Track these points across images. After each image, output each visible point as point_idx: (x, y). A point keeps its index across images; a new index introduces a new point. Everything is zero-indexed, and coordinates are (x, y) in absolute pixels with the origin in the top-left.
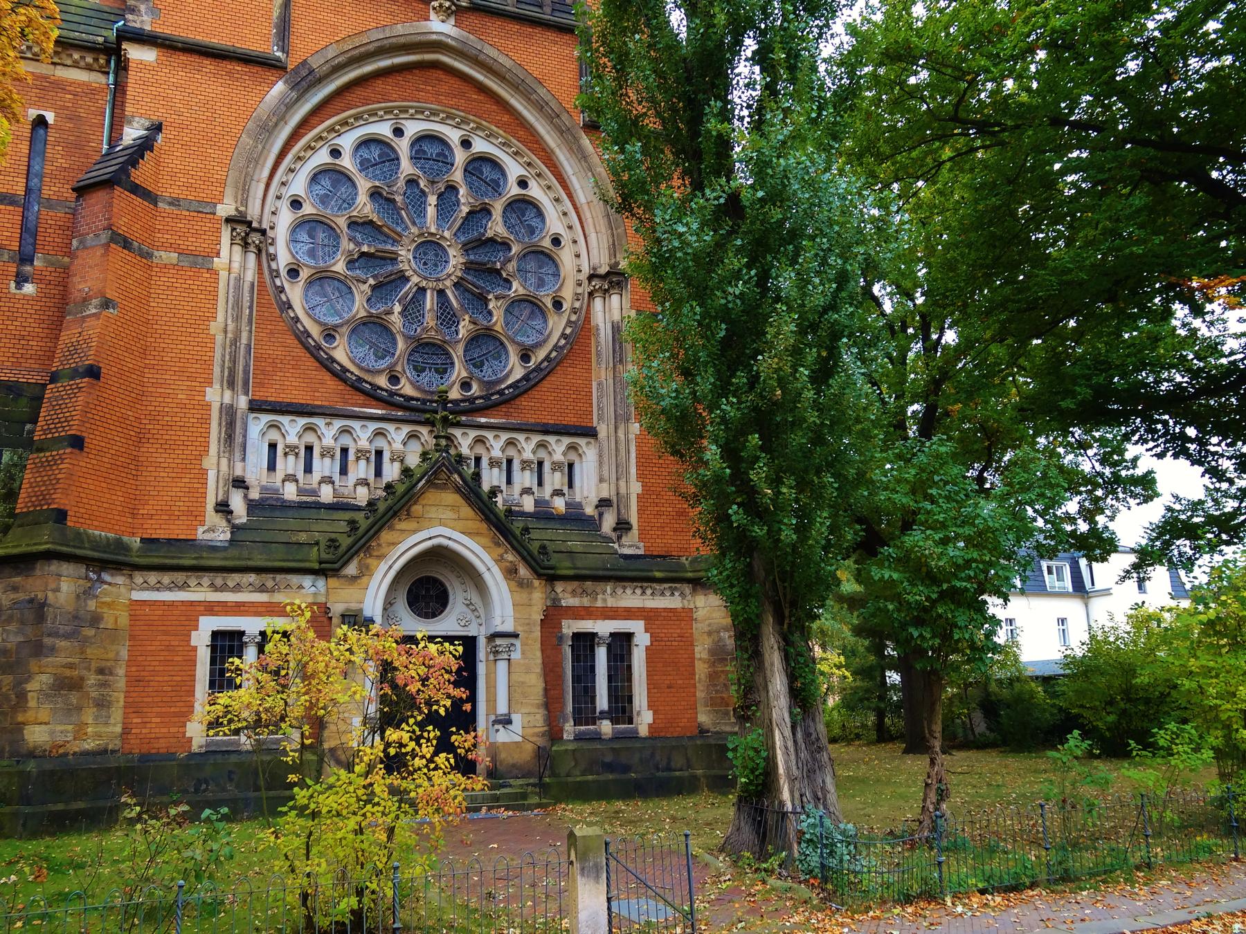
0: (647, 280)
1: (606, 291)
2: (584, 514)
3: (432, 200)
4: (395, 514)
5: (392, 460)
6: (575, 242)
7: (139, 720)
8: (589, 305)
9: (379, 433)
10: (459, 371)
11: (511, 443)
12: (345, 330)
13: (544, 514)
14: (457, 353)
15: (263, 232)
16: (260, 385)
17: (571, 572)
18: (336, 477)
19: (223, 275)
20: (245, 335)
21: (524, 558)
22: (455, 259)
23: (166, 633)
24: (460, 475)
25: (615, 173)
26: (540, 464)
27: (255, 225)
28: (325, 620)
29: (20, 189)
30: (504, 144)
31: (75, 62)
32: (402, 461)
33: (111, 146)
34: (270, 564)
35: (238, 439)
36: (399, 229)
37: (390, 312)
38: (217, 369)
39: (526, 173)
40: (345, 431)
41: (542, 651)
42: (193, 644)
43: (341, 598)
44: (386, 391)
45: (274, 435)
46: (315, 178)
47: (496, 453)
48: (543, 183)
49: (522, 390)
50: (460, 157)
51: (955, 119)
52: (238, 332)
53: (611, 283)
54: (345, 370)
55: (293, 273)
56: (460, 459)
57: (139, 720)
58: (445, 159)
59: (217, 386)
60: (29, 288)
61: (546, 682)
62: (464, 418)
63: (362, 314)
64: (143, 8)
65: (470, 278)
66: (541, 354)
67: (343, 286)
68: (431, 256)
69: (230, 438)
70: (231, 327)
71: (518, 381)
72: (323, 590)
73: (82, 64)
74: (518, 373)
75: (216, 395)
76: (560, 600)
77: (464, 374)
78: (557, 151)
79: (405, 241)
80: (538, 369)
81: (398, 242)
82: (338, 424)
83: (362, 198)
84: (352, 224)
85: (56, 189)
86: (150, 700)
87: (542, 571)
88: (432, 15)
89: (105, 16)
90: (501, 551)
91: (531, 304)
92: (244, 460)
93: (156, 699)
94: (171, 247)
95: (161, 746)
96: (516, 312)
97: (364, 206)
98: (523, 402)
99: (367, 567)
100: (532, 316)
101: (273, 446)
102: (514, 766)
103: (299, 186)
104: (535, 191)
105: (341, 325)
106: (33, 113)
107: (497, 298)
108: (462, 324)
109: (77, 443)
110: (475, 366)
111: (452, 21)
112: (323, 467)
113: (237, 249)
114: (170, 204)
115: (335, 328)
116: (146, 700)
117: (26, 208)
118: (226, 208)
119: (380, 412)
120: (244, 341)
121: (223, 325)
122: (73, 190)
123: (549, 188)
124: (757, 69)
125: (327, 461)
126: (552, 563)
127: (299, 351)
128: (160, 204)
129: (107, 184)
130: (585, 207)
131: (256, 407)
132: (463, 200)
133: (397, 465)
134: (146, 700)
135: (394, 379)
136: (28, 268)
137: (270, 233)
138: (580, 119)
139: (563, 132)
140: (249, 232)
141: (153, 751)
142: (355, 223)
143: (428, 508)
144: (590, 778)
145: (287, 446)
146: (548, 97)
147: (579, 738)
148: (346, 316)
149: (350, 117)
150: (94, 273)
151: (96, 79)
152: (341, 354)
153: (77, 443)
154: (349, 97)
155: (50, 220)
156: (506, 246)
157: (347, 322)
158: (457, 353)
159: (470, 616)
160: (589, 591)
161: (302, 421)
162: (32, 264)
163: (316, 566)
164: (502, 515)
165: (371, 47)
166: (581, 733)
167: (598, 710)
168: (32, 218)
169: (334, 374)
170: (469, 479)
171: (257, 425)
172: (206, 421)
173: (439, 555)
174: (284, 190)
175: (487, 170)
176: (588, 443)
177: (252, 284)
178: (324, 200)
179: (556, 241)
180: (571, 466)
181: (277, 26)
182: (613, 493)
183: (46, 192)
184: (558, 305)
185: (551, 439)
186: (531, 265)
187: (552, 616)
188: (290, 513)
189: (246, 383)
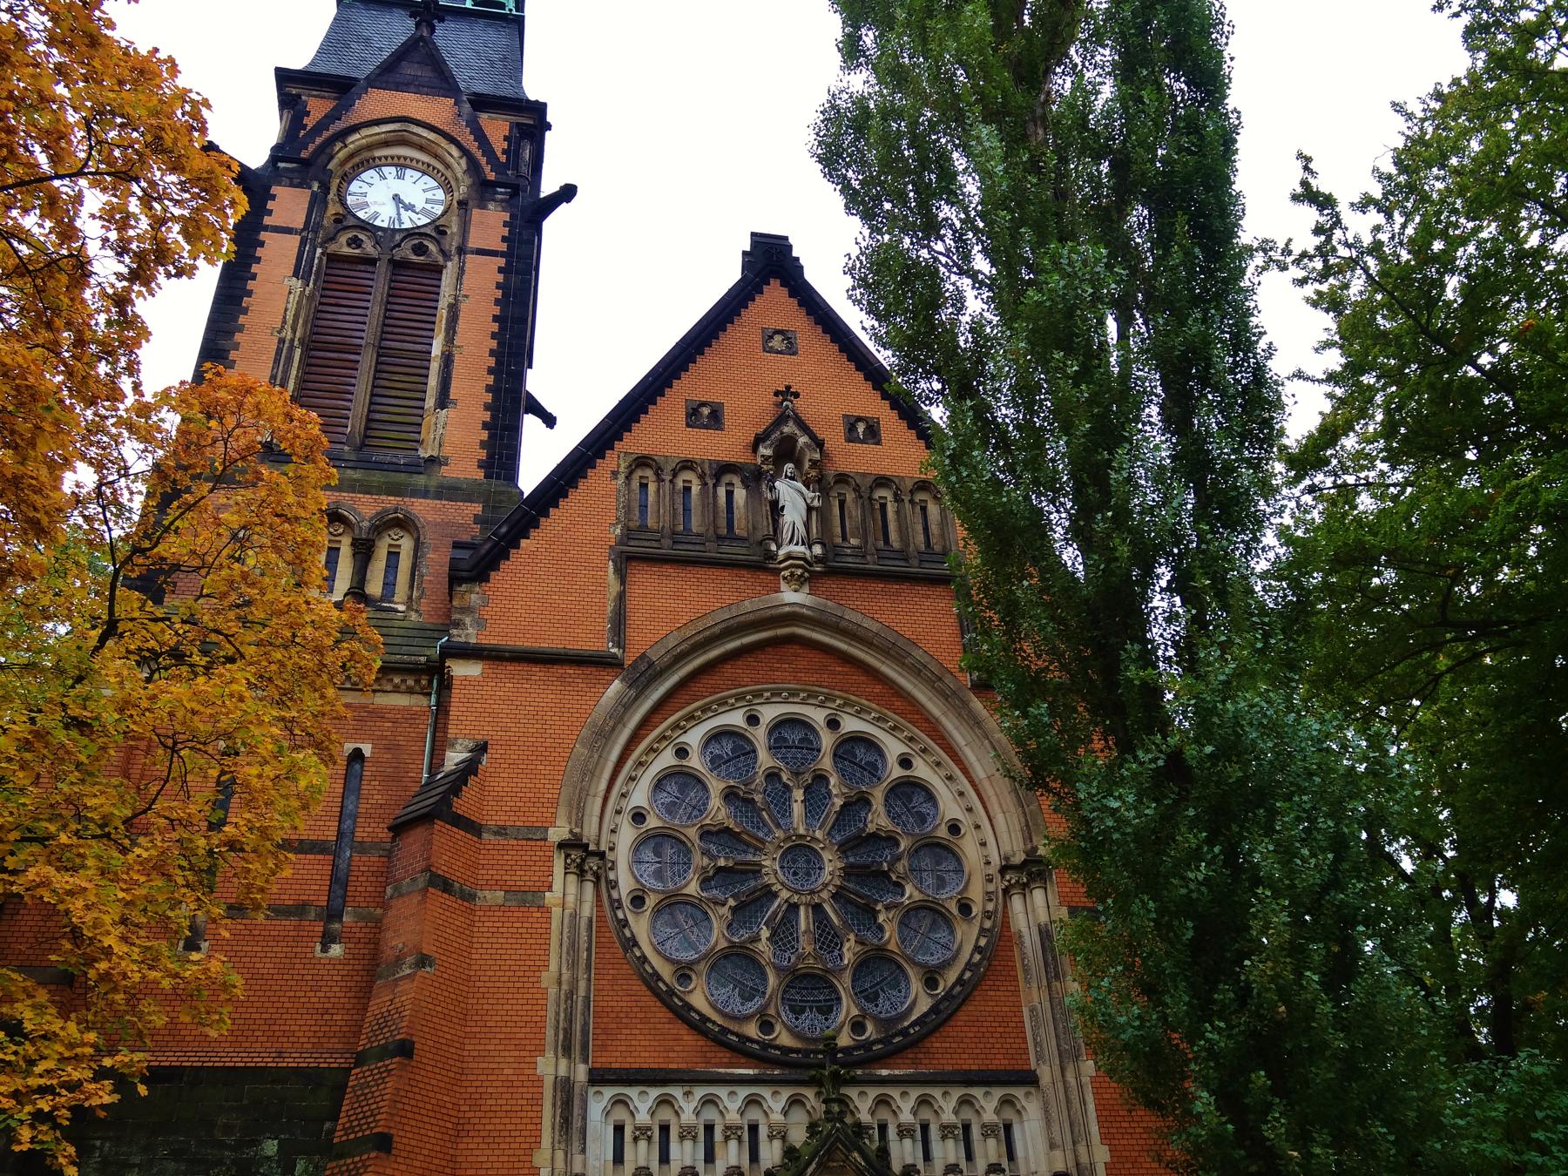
0: (1076, 870)
1: (1025, 886)
3: (798, 794)
5: (771, 1138)
6: (978, 827)
8: (1005, 906)
9: (752, 1101)
10: (848, 1008)
11: (924, 1101)
12: (703, 967)
14: (844, 984)
15: (602, 855)
16: (603, 1047)
19: (556, 911)
20: (582, 985)
22: (831, 864)
25: (1019, 742)
26: (967, 1128)
27: (592, 847)
29: (331, 835)
30: (878, 719)
31: (396, 686)
32: (784, 1138)
33: (432, 774)
35: (577, 1124)
36: (761, 834)
37: (757, 939)
38: (550, 1033)
39: (906, 750)
40: (709, 1101)
44: (757, 1042)
45: (620, 1114)
46: (659, 785)
47: (906, 1117)
48: (930, 759)
49: (931, 1027)
50: (827, 740)
51: (1445, 623)
52: (574, 982)
53: (1029, 874)
55: (638, 901)
56: (860, 1129)
58: (810, 745)
59: (550, 1054)
60: (336, 950)
62: (859, 1072)
63: (723, 944)
64: (468, 620)
65: (851, 885)
66: (952, 976)
67: (698, 911)
68: (801, 863)
69: (566, 1122)
70: (565, 977)
71: (925, 1015)
73: (403, 687)
74: (924, 1005)
75: (549, 1066)
77: (855, 1012)
78: (944, 720)
79: (769, 848)
80: (949, 995)
81: (760, 850)
82: (700, 1092)
83: (715, 802)
84: (705, 834)
85: (371, 830)
88: (783, 586)
89: (428, 633)
91: (931, 911)
92: (583, 1151)
94: (497, 884)
96: (914, 925)
97: (717, 811)
98: (935, 1044)
100: (934, 927)
101: (619, 1129)
103: (640, 796)
104: (921, 770)
105: (698, 961)
106: (349, 747)
107: (888, 908)
108: (847, 945)
109: (383, 1143)
110: (867, 999)
111: (806, 589)
113: (572, 878)
114: (496, 833)
115: (690, 965)
117: (336, 854)
118: (558, 833)
119: (751, 1072)
120: (582, 992)
121: (556, 975)
122: (390, 829)
123: (938, 764)
124: (1177, 600)
125: (688, 1144)
127: (649, 1000)
128: (485, 835)
129: (426, 818)
130: (986, 784)
131: (599, 1078)
132: (834, 792)
133: (777, 1144)
135: (766, 1026)
136: (337, 926)
137: (610, 856)
138: (967, 679)
139: (950, 697)
140: (585, 858)
142: (708, 832)
145: (637, 1128)
146: (925, 659)
148: (703, 949)
149: (696, 710)
150: (411, 924)
151: (418, 702)
152: (698, 1000)
153: (383, 1143)
154: (695, 688)
155: (363, 865)
156: (892, 841)
157: (705, 957)
158: (844, 984)
161: (654, 1093)
162: (341, 921)
165: (716, 630)
168: (343, 866)
170: (873, 1156)
171: (598, 1104)
172: (537, 1101)
174: (624, 803)
175: (860, 753)
176: (1028, 1094)
177: (590, 920)
178: (671, 809)
179: (954, 828)
180: (1008, 1128)
181: (611, 621)
182: (1071, 1164)
183: (360, 834)
184: (965, 908)
185: (977, 1092)
186: (926, 862)
189: (585, 1047)
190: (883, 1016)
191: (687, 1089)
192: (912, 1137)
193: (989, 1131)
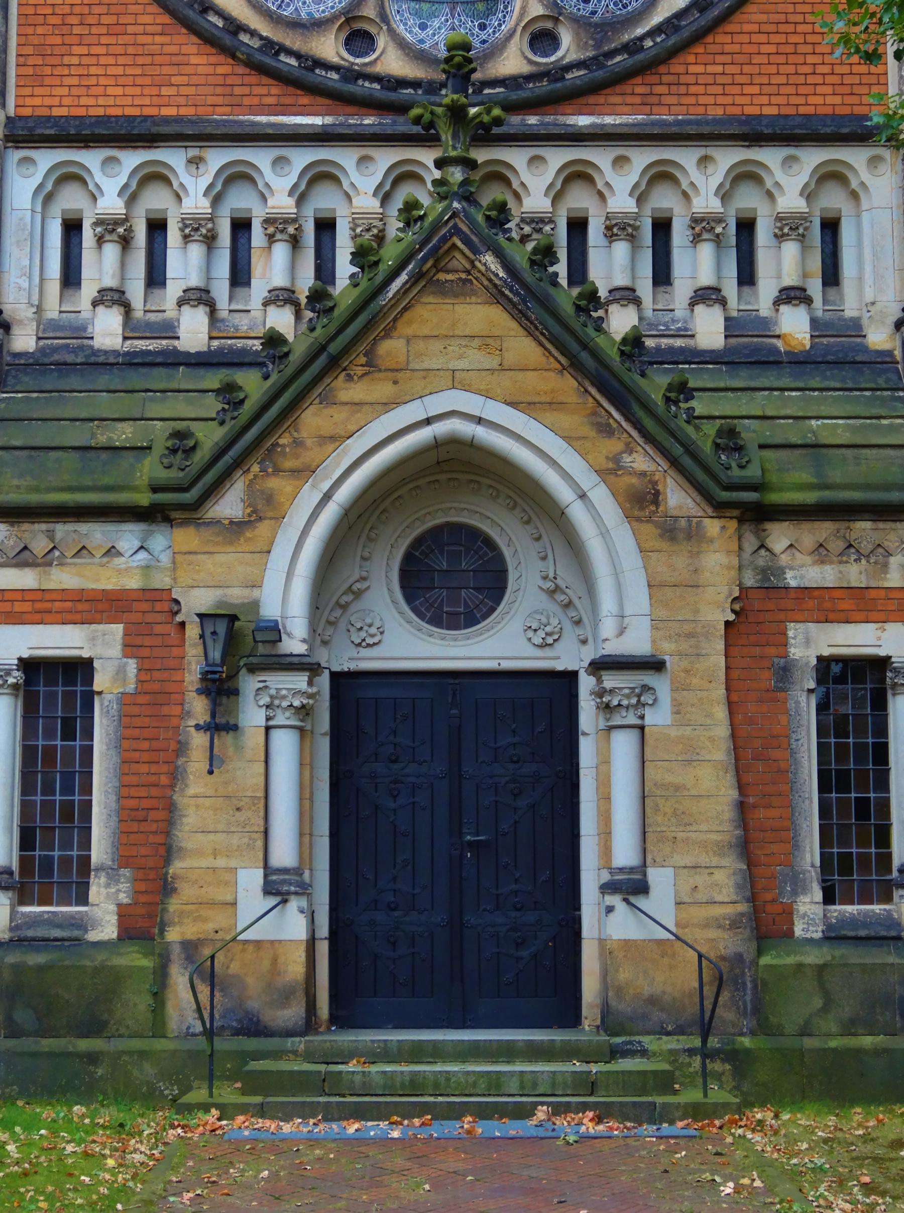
2: (865, 349)
4: (334, 364)
13: (751, 354)
17: (810, 497)
18: (221, 290)
21: (674, 463)
24: (499, 254)
34: (34, 498)
41: (732, 707)
43: (197, 574)
44: (336, 68)
49: (685, 34)
54: (235, 27)
61: (741, 787)
62: (533, 120)
72: (165, 559)
76: (781, 571)
77: (537, 10)
82: (218, 158)
87: (725, 495)
90: (614, 445)
98: (692, 65)
99: (269, 499)
101: (72, 228)
102: (653, 1001)
112: (184, 265)
119: (318, 121)
126: (753, 472)
135: (359, 39)
143: (420, 345)
144: (867, 1041)
147: (834, 936)
159: (557, 618)
160: (866, 547)
161: (132, 159)
163: (144, 499)
164: (613, 354)
166: (846, 922)
167: (896, 863)
169: (208, 39)
173: (452, 464)
176: (874, 161)
185: (770, 157)
187: (757, 615)
188: (104, 380)
190: (595, 19)
191: (193, 152)
192: (633, 239)
193: (789, 227)
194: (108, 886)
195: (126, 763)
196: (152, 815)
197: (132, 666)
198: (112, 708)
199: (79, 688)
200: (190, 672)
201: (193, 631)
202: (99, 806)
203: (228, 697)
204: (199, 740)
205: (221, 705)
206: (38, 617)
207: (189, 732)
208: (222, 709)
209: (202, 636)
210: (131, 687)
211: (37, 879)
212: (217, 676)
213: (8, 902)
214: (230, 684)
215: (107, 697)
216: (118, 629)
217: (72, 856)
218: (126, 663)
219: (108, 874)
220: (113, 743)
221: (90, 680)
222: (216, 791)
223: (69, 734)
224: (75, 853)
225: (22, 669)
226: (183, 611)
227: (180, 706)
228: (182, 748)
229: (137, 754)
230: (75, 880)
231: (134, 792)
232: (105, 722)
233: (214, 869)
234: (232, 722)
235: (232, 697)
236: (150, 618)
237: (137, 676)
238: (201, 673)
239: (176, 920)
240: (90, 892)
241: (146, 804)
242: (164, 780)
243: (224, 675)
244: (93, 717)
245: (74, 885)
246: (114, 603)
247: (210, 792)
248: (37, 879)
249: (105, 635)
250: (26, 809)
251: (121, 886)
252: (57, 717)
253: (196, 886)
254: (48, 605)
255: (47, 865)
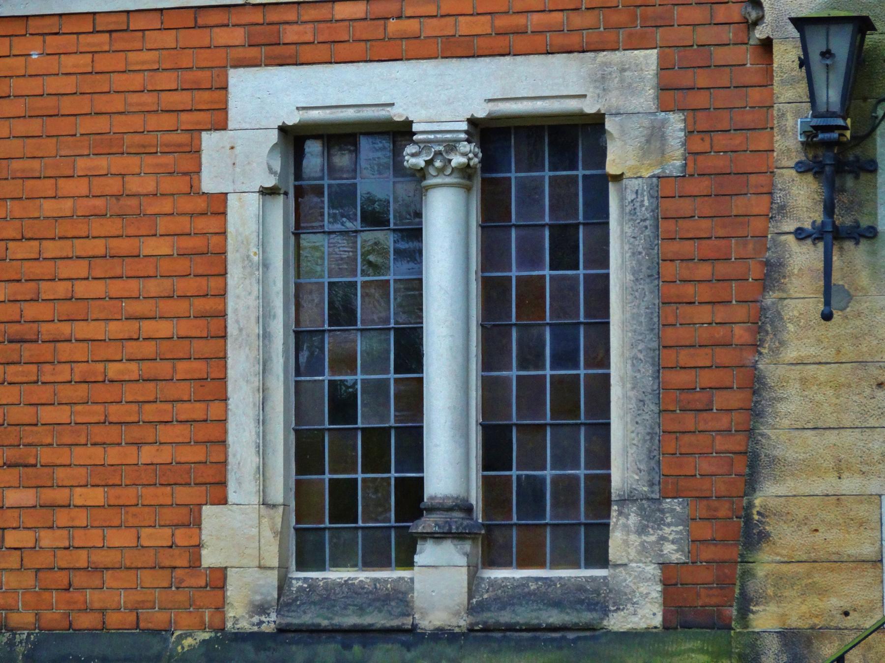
7: (27, 497)
23: (107, 145)
28: (748, 57)
42: (209, 184)
57: (27, 497)
86: (61, 414)
93: (85, 414)
95: (114, 601)
116: (47, 414)
134: (47, 414)
141: (85, 621)
194: (642, 530)
195: (668, 304)
196: (720, 400)
197: (675, 123)
198: (642, 205)
199: (580, 172)
200: (783, 132)
201: (786, 55)
202: (623, 386)
203: (857, 177)
204: (804, 258)
205: (843, 190)
206: (501, 43)
207: (784, 244)
208: (845, 198)
209: (804, 63)
210: (675, 164)
211: (515, 520)
212: (835, 135)
213: (463, 561)
214: (858, 151)
215: (633, 184)
216: (648, 60)
217: (576, 478)
218: (664, 122)
219: (642, 508)
220: (644, 269)
221: (599, 155)
222: (838, 351)
223: (564, 253)
224: (581, 472)
225: (476, 138)
226: (768, 18)
227: (766, 198)
228: (772, 273)
229: (689, 289)
230: (583, 520)
231: (684, 357)
232: (628, 230)
233: (839, 498)
234: (865, 222)
235: (864, 177)
236: (705, 35)
237: (684, 144)
238: (804, 133)
239: (770, 592)
240: (611, 543)
241: (707, 379)
242: (740, 334)
243: (848, 134)
244: (607, 224)
245: (583, 529)
246: (639, 11)
247: (828, 354)
248: (515, 520)
249: (623, 70)
250: (492, 394)
251: (667, 530)
252: (544, 226)
253: (805, 529)
254: (521, 20)
255: (532, 493)
